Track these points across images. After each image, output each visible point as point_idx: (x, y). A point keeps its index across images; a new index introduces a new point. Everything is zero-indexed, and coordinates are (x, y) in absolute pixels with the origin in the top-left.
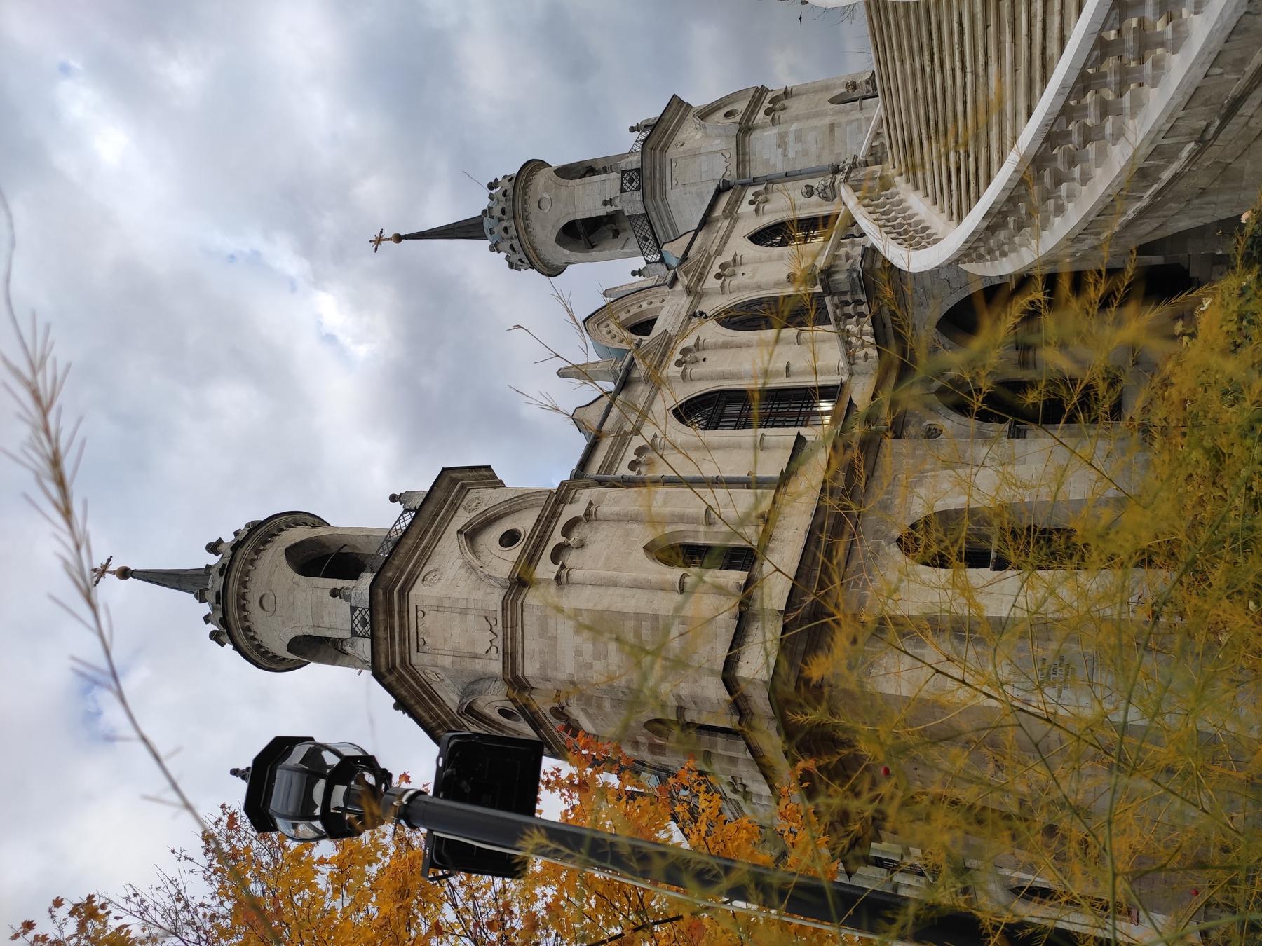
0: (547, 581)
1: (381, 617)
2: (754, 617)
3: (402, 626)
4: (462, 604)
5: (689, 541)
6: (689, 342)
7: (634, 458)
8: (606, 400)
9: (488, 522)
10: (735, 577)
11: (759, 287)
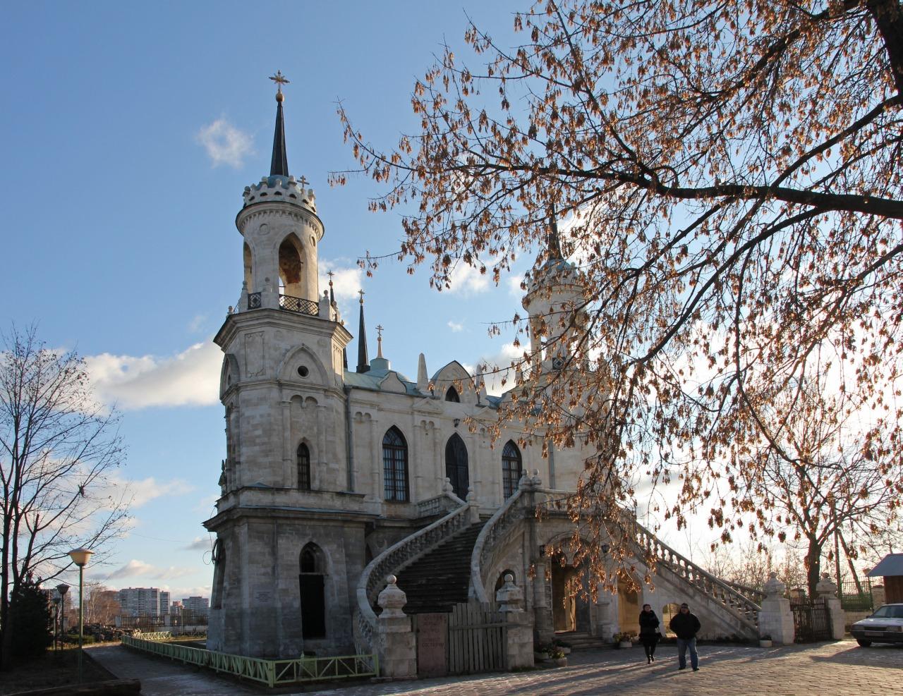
0: (282, 398)
1: (256, 315)
2: (273, 494)
3: (254, 325)
4: (267, 356)
5: (311, 456)
6: (438, 422)
7: (363, 414)
8: (402, 389)
9: (312, 356)
10: (292, 481)
11: (474, 452)
